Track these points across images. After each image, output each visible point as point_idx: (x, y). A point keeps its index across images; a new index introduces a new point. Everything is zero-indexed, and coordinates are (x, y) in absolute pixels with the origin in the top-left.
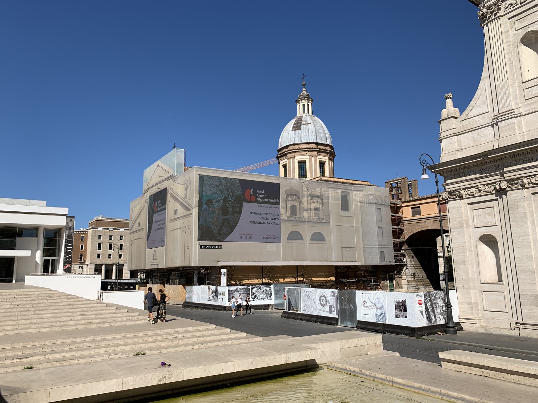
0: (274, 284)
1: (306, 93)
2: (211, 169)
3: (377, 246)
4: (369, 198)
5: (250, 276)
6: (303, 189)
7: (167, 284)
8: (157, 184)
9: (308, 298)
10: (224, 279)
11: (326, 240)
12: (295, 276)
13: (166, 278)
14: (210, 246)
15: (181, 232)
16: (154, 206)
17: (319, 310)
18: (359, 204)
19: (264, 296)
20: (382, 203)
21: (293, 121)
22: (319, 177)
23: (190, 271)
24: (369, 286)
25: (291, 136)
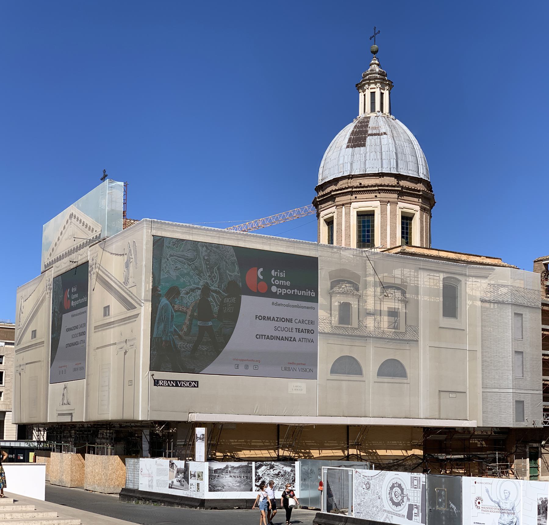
0: (300, 460)
1: (377, 69)
2: (179, 226)
3: (511, 391)
4: (500, 293)
5: (253, 444)
6: (365, 270)
7: (89, 453)
8: (70, 253)
9: (368, 489)
10: (200, 448)
11: (408, 375)
12: (343, 445)
13: (88, 441)
14: (173, 381)
15: (118, 352)
16: (63, 297)
17: (389, 512)
18: (479, 303)
19: (280, 483)
20: (525, 302)
21: (350, 128)
22: (400, 246)
23: (134, 428)
24: (489, 469)
25: (344, 158)
